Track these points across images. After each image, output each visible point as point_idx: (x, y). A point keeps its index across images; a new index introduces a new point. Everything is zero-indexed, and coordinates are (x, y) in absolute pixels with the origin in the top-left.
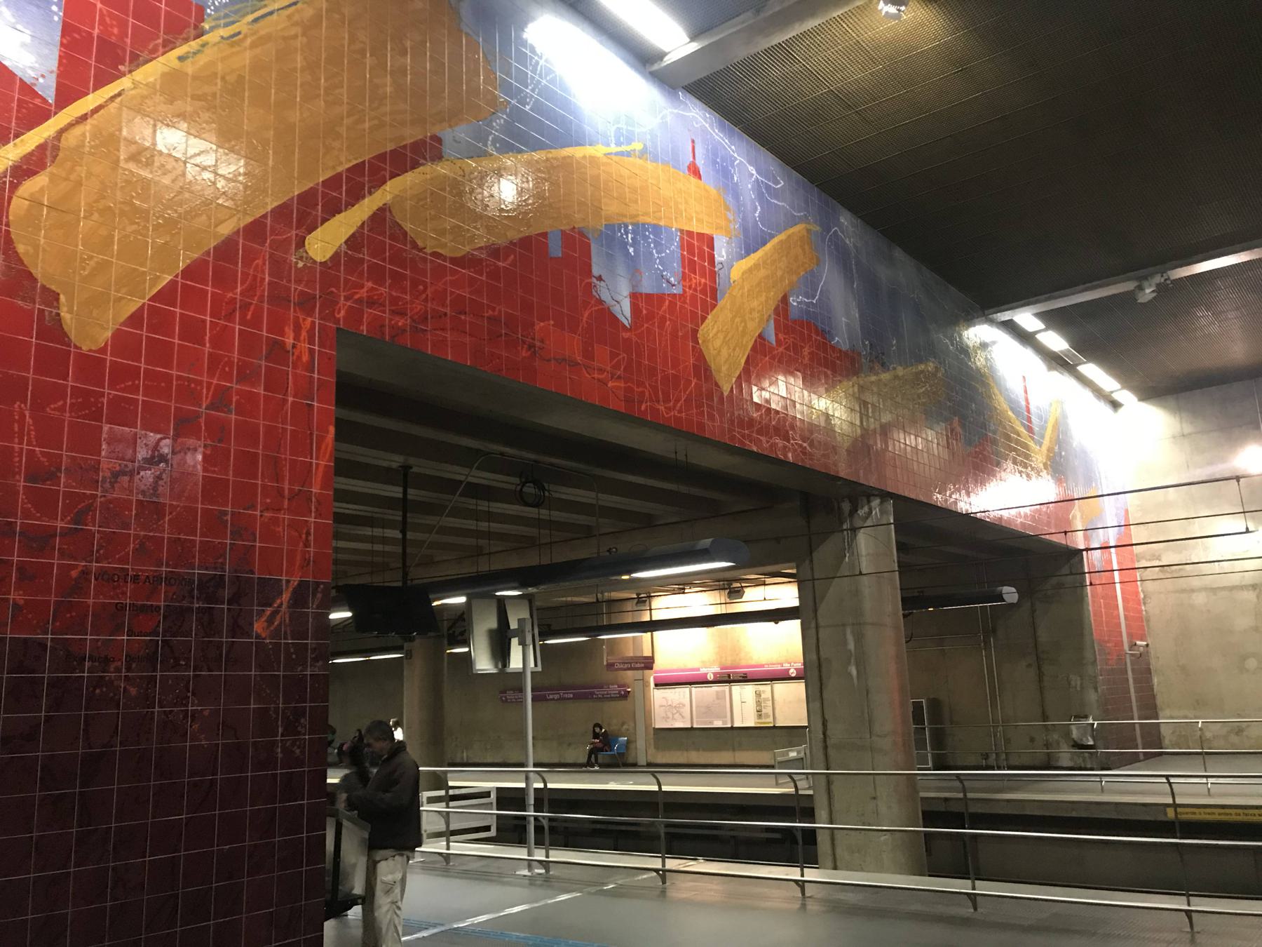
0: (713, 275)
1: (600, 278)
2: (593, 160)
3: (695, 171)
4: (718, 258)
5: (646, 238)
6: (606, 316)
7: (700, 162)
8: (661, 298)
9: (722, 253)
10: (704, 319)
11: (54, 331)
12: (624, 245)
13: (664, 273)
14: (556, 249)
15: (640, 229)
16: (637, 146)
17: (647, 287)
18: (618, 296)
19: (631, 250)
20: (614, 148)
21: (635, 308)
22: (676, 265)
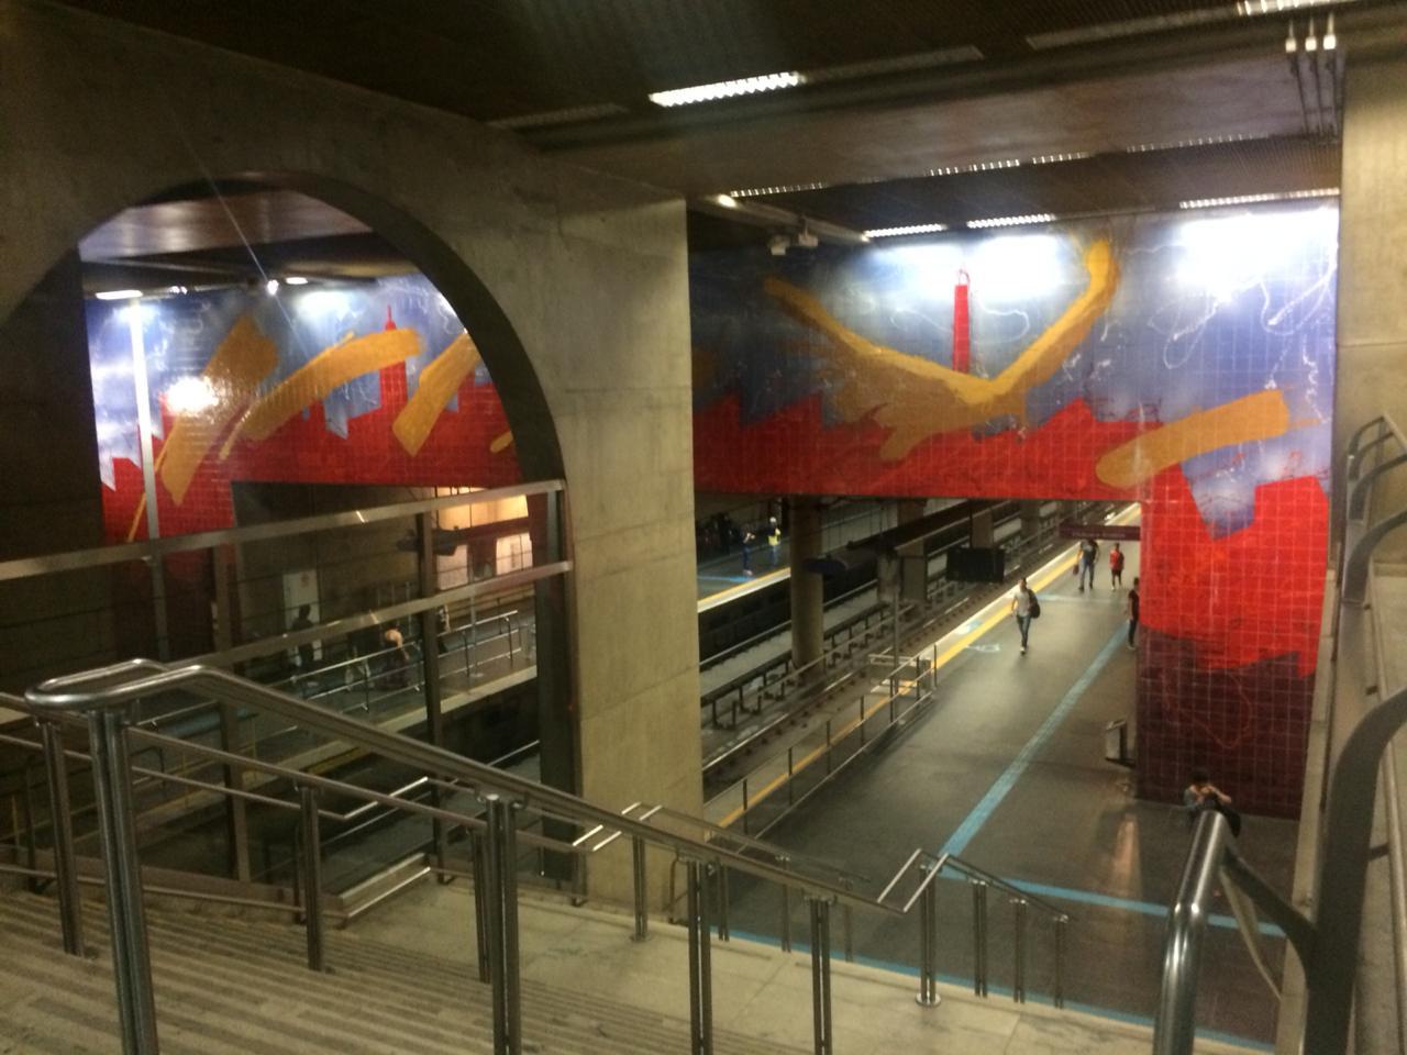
0: (404, 386)
1: (330, 420)
2: (325, 361)
3: (391, 326)
4: (408, 373)
5: (356, 386)
6: (335, 438)
7: (395, 318)
8: (366, 417)
9: (411, 369)
10: (397, 415)
11: (172, 502)
12: (343, 396)
13: (370, 399)
14: (306, 416)
15: (352, 383)
16: (350, 335)
17: (357, 412)
18: (340, 425)
19: (347, 398)
20: (336, 345)
21: (350, 428)
22: (377, 393)
